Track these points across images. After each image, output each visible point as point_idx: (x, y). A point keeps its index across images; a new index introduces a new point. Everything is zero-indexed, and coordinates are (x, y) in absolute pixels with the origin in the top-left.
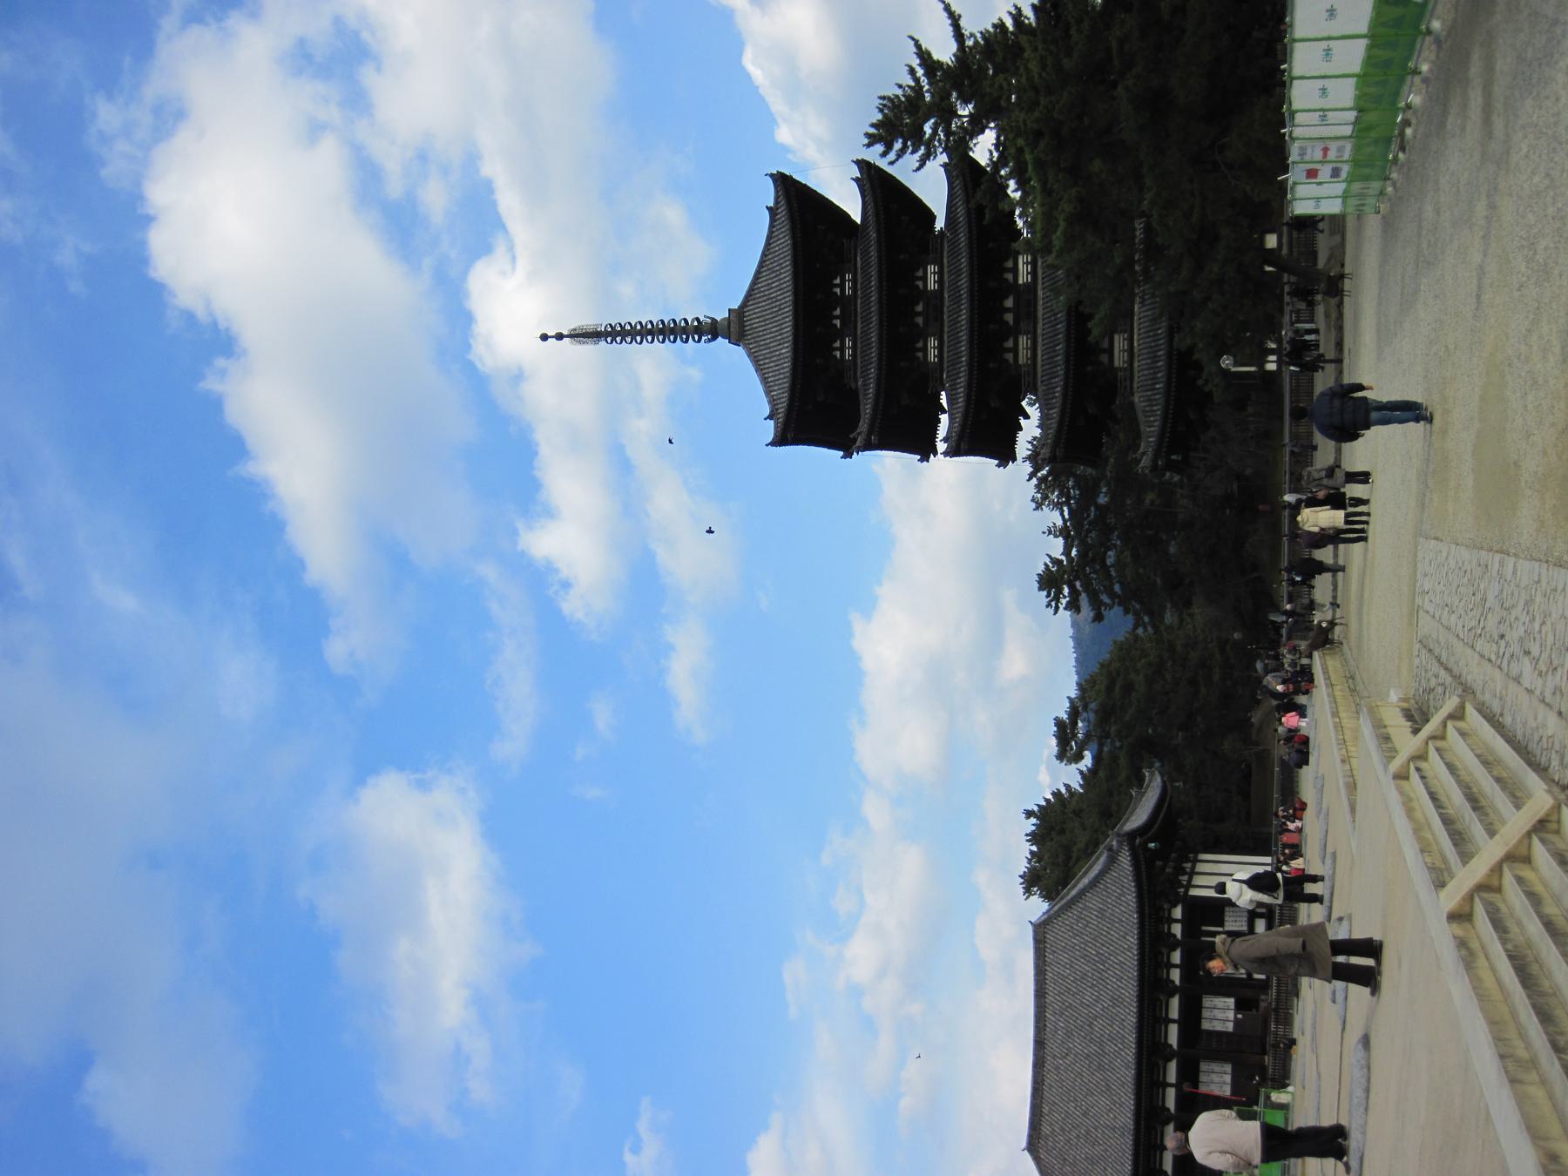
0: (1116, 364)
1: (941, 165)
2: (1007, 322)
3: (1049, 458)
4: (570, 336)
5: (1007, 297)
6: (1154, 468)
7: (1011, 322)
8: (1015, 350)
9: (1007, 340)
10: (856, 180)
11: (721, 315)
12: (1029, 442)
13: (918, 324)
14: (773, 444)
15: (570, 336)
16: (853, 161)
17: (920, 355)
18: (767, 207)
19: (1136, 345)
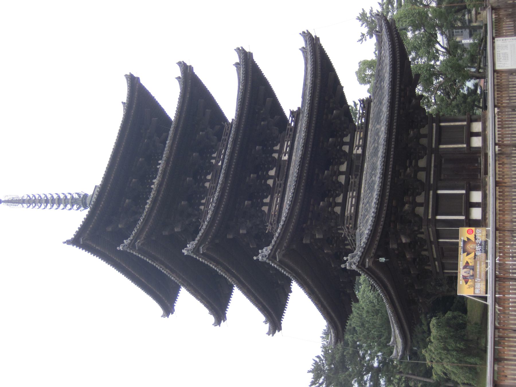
0: (346, 214)
1: (234, 65)
2: (269, 185)
3: (269, 255)
4: (5, 202)
5: (272, 169)
6: (361, 264)
7: (271, 185)
8: (270, 205)
9: (266, 197)
10: (178, 78)
11: (90, 192)
12: (314, 360)
13: (206, 187)
14: (68, 242)
15: (5, 202)
16: (177, 63)
17: (202, 207)
18: (122, 102)
19: (362, 191)
